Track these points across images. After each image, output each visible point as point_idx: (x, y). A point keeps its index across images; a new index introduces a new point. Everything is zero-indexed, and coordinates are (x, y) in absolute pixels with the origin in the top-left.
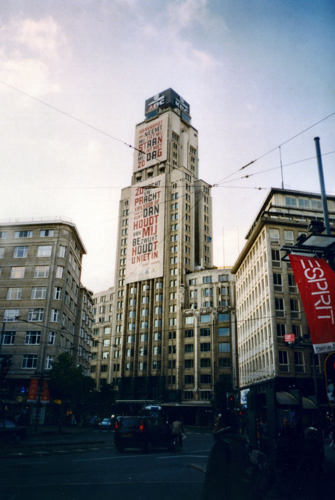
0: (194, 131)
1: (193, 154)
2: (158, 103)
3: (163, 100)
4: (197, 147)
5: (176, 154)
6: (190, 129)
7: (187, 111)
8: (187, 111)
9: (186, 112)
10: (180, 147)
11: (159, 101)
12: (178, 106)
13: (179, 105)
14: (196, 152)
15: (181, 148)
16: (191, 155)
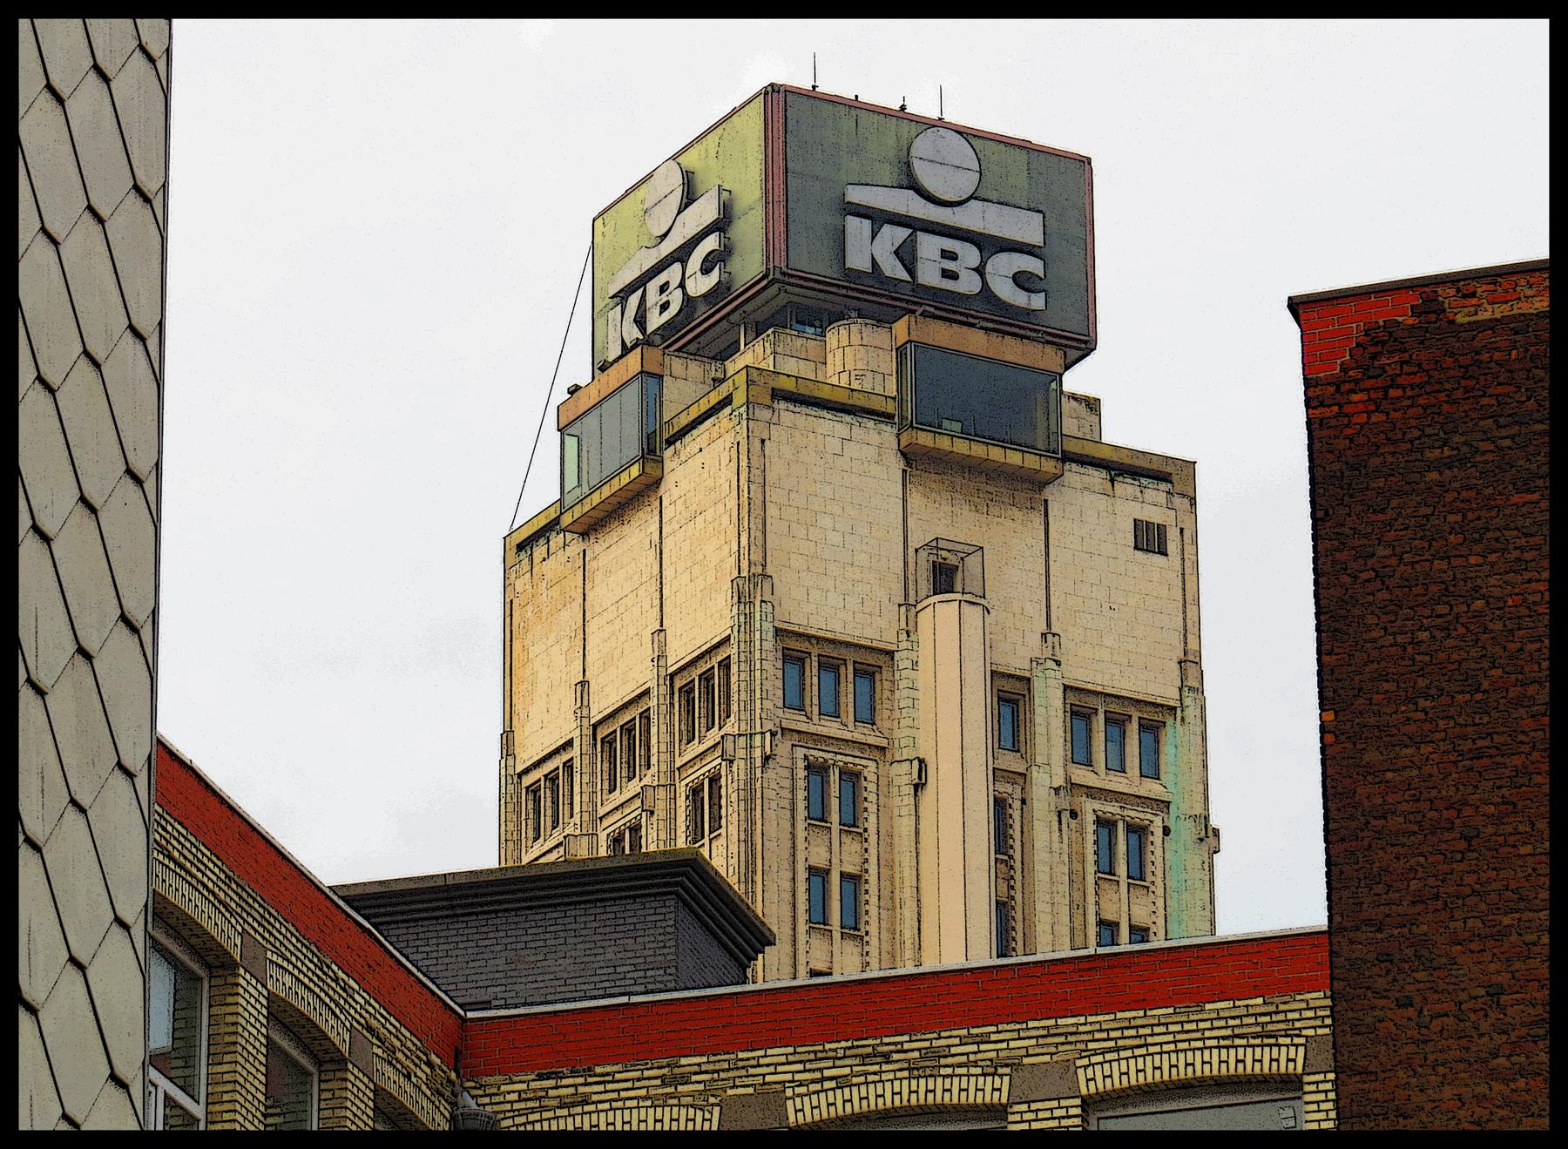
0: (1126, 488)
1: (1117, 783)
2: (673, 274)
3: (711, 243)
4: (1189, 662)
5: (853, 881)
6: (1050, 493)
7: (1033, 265)
8: (1033, 265)
9: (1022, 280)
10: (903, 775)
11: (681, 255)
12: (893, 269)
13: (906, 255)
14: (1172, 737)
15: (918, 787)
16: (1089, 808)
